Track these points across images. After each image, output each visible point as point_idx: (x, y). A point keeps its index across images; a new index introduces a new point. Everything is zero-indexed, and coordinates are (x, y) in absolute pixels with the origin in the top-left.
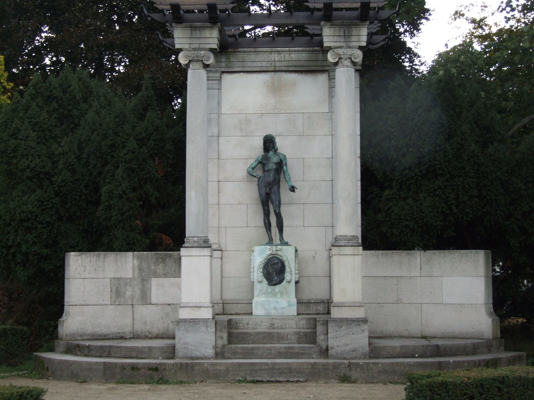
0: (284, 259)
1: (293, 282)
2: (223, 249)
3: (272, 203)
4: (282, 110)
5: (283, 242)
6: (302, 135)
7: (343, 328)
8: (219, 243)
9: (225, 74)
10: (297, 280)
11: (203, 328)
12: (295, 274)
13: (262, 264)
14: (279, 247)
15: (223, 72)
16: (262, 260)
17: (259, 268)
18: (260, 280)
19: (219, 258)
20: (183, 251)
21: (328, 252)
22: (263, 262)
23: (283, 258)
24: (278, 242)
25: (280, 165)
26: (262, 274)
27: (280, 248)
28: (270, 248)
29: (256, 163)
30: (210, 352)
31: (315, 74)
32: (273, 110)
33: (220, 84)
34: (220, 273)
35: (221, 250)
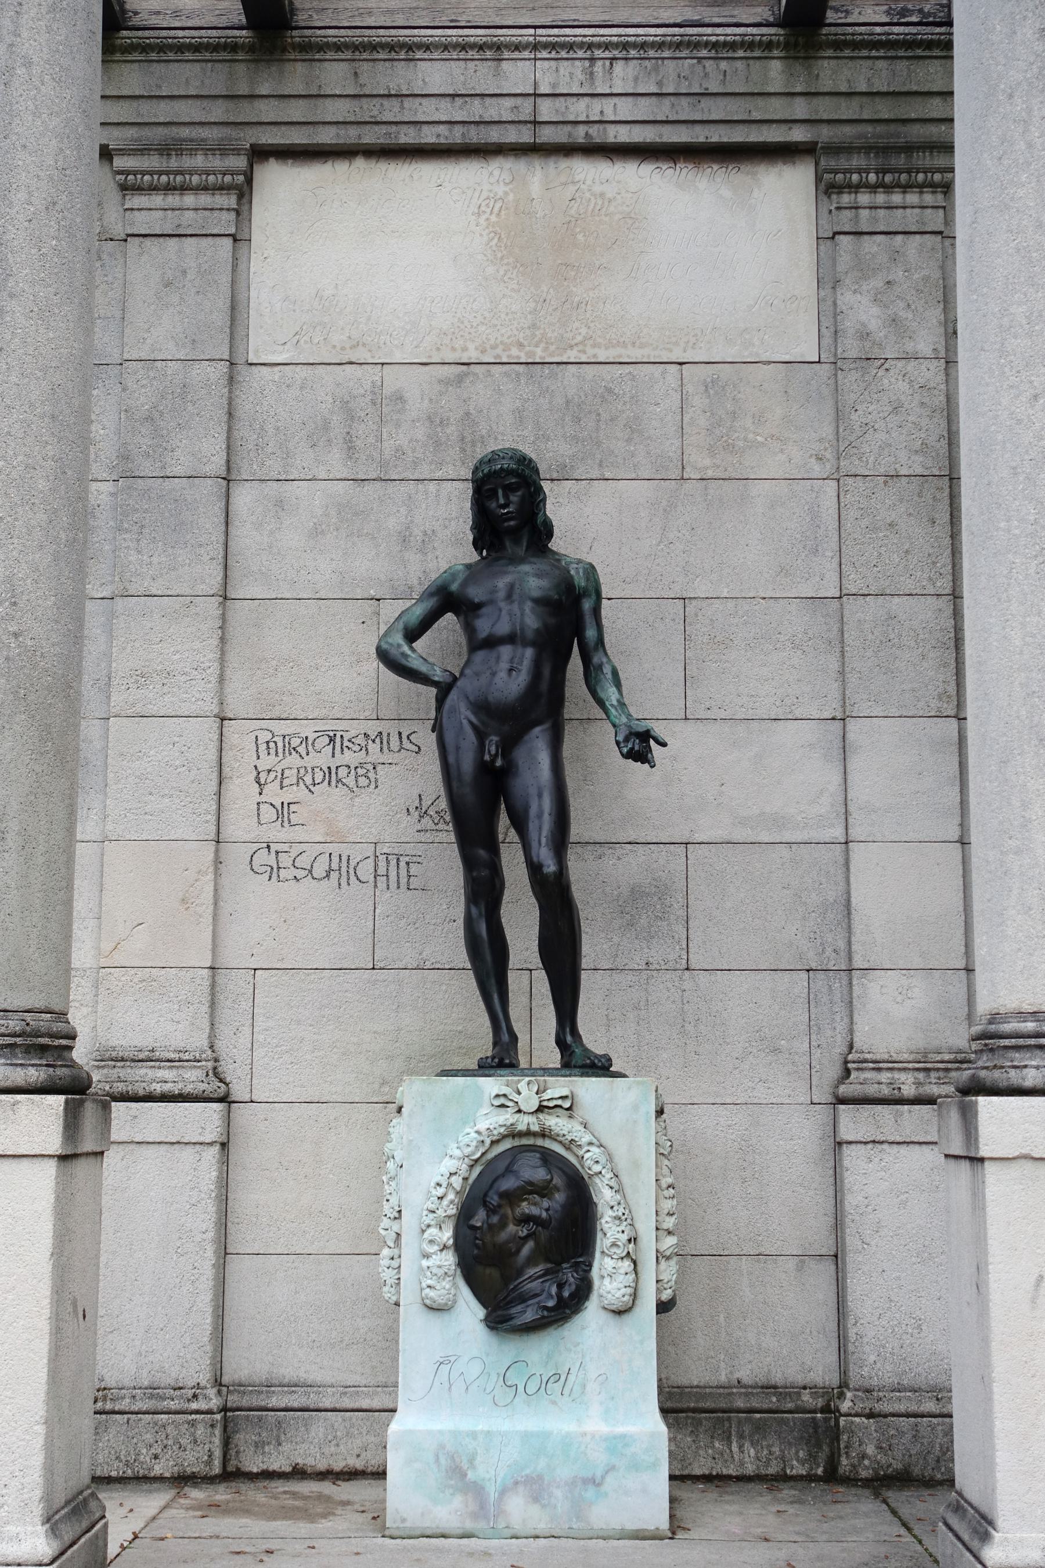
0: (591, 1161)
2: (238, 1091)
3: (519, 823)
4: (571, 347)
5: (578, 1059)
6: (676, 473)
8: (216, 1060)
9: (272, 160)
10: (666, 1296)
12: (660, 1256)
13: (451, 1196)
14: (558, 1088)
15: (260, 154)
17: (429, 1219)
19: (211, 1144)
21: (822, 1114)
22: (457, 1182)
24: (553, 1057)
26: (449, 1260)
27: (565, 1092)
28: (505, 1090)
31: (747, 167)
32: (521, 345)
33: (242, 211)
34: (211, 1235)
35: (221, 1100)
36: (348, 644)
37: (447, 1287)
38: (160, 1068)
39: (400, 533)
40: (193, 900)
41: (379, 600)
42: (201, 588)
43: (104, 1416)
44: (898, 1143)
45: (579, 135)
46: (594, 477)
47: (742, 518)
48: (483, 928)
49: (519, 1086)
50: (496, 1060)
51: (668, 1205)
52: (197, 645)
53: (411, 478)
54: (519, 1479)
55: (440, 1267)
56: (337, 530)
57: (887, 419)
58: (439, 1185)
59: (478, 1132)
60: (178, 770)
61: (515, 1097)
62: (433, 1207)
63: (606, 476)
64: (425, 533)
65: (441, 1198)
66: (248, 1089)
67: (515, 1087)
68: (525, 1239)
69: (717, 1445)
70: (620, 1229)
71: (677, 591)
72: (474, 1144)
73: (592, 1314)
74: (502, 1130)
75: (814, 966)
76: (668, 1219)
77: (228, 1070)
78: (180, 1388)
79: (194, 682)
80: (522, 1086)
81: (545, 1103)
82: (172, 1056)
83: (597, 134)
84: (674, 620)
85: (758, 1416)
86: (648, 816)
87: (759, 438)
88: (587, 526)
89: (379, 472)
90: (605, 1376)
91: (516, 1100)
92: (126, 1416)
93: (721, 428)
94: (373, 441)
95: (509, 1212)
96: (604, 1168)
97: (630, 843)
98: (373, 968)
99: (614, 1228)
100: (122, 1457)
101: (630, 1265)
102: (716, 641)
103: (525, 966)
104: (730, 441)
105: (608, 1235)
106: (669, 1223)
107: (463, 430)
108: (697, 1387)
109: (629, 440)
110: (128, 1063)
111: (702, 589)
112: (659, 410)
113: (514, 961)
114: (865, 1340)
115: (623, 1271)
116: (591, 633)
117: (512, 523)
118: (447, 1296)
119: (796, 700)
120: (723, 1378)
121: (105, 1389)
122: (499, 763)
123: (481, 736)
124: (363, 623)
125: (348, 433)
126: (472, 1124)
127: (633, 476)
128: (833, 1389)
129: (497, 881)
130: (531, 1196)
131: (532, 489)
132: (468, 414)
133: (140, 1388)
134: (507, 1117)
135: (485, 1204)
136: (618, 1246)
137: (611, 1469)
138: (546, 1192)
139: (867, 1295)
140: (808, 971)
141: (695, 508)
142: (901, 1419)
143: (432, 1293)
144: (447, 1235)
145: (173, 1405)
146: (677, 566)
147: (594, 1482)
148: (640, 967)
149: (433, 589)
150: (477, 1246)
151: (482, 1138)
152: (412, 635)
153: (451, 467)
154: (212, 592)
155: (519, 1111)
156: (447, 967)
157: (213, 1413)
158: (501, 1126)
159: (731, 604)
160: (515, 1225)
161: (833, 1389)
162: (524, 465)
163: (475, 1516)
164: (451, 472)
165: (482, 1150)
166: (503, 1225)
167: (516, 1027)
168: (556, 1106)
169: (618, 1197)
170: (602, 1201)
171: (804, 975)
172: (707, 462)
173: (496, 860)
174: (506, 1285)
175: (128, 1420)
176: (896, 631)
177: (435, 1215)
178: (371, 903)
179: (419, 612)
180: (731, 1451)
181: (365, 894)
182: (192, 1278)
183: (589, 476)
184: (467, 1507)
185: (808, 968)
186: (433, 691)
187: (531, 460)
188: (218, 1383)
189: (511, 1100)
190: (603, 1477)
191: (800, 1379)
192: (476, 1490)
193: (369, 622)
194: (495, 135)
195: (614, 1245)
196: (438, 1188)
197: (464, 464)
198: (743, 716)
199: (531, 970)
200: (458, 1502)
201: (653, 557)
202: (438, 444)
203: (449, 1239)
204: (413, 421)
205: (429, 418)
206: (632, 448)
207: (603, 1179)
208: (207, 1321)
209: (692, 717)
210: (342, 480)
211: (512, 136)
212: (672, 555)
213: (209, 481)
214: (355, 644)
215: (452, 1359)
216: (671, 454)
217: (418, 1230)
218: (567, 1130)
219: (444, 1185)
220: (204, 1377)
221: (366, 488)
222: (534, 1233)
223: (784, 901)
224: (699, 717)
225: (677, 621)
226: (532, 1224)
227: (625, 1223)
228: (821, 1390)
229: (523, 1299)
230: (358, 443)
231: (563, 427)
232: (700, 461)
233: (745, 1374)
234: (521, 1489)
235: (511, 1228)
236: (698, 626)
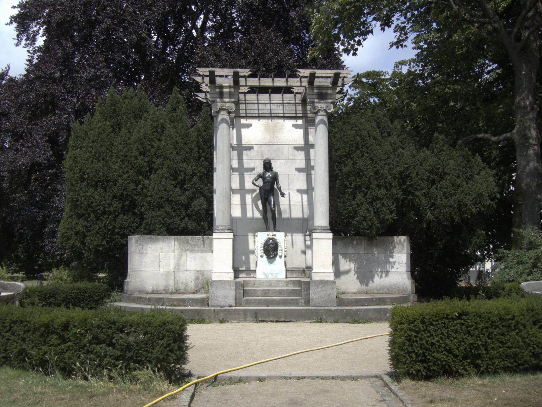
1: (283, 257)
7: (320, 287)
11: (228, 287)
18: (262, 254)
20: (215, 235)
25: (275, 178)
30: (233, 302)
45: (276, 115)
73: (278, 257)
83: (278, 115)
111: (290, 173)
152: (256, 181)
192: (266, 274)
194: (265, 115)
211: (267, 115)
232: (290, 157)
233: (294, 266)
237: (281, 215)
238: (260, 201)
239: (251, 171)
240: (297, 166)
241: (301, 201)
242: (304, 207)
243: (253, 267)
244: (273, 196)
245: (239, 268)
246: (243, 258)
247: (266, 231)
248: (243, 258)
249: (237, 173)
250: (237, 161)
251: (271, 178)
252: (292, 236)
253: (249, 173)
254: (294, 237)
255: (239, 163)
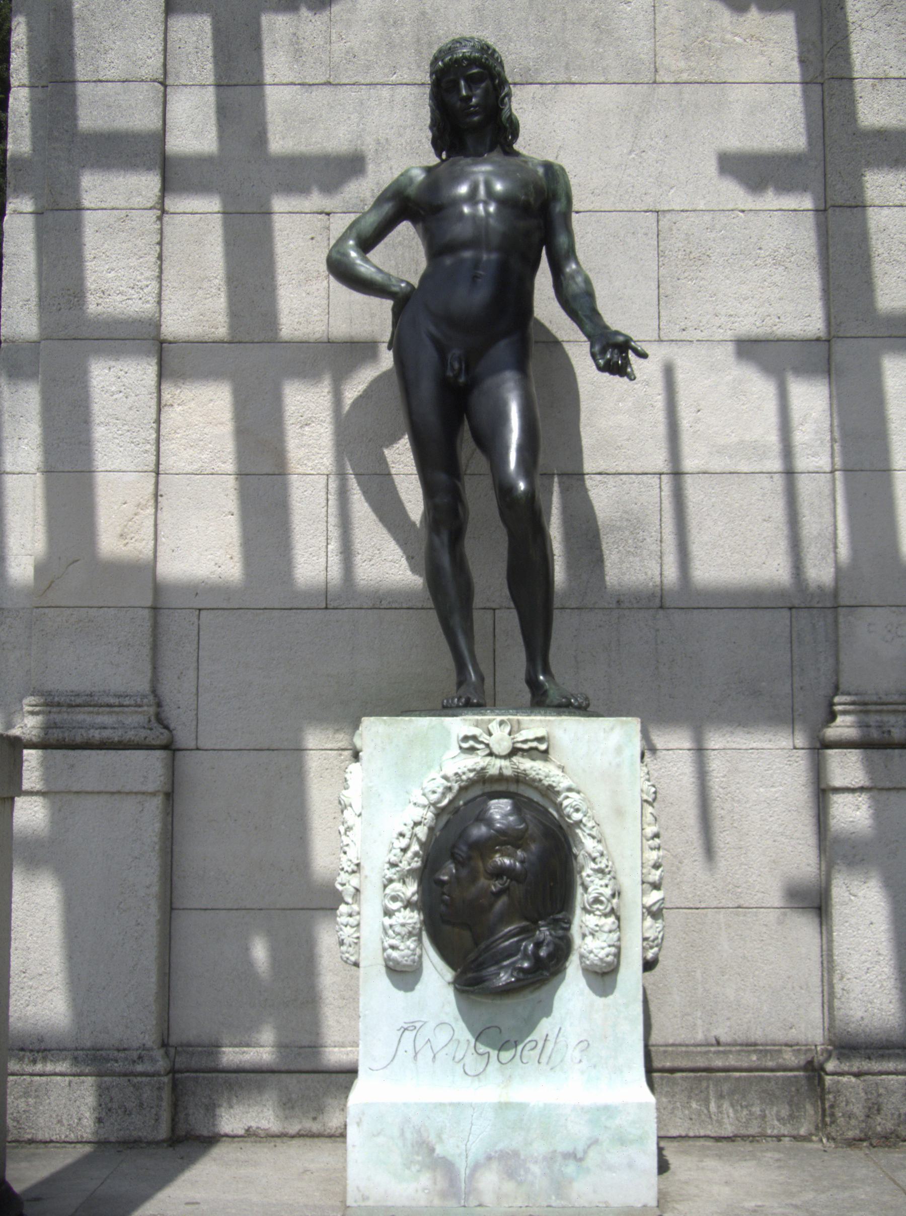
1: (631, 971)
2: (184, 738)
6: (648, 76)
10: (650, 955)
13: (415, 847)
16: (418, 814)
17: (391, 873)
18: (405, 950)
19: (154, 794)
22: (422, 832)
23: (559, 807)
26: (413, 917)
27: (540, 733)
28: (476, 731)
29: (387, 208)
34: (155, 889)
35: (165, 747)
36: (297, 262)
37: (412, 946)
38: (98, 713)
39: (351, 141)
40: (133, 535)
41: (328, 214)
42: (137, 201)
43: (44, 1078)
44: (889, 789)
46: (560, 80)
47: (719, 125)
48: (445, 560)
49: (490, 726)
50: (463, 700)
51: (653, 856)
52: (134, 262)
53: (363, 82)
54: (493, 1154)
55: (403, 925)
56: (284, 138)
57: (876, 18)
58: (402, 835)
59: (446, 778)
60: (115, 397)
61: (484, 738)
62: (394, 859)
63: (574, 80)
64: (378, 142)
65: (404, 850)
66: (194, 736)
67: (485, 726)
68: (498, 894)
69: (694, 1105)
70: (603, 882)
71: (649, 203)
72: (440, 790)
74: (471, 775)
75: (796, 603)
76: (654, 871)
77: (172, 715)
78: (125, 1049)
79: (130, 302)
80: (494, 727)
81: (519, 745)
82: (112, 701)
84: (646, 234)
85: (737, 1074)
86: (619, 444)
87: (737, 39)
88: (553, 133)
89: (328, 76)
90: (586, 1043)
91: (486, 741)
92: (67, 1078)
93: (696, 28)
94: (322, 43)
95: (480, 864)
96: (585, 816)
97: (600, 474)
98: (326, 608)
99: (597, 881)
100: (65, 1121)
101: (614, 923)
102: (692, 256)
103: (488, 605)
104: (706, 42)
105: (590, 890)
106: (655, 875)
107: (418, 30)
108: (673, 1045)
109: (598, 41)
110: (64, 709)
112: (629, 9)
113: (478, 601)
114: (852, 995)
115: (606, 928)
116: (562, 240)
117: (476, 119)
118: (412, 957)
119: (777, 320)
120: (700, 1037)
121: (45, 1050)
122: (462, 380)
123: (441, 350)
124: (312, 239)
125: (295, 34)
126: (438, 768)
127: (602, 79)
128: (816, 1046)
129: (460, 508)
130: (504, 847)
131: (497, 81)
132: (423, 13)
133: (82, 1049)
134: (478, 761)
135: (453, 857)
136: (601, 902)
137: (594, 1142)
138: (520, 842)
139: (853, 949)
140: (790, 608)
141: (668, 114)
142: (891, 1077)
143: (395, 954)
144: (410, 889)
145: (117, 1067)
146: (650, 176)
147: (573, 1156)
148: (611, 606)
149: (388, 194)
150: (443, 901)
151: (449, 784)
152: (367, 244)
153: (405, 70)
154: (149, 205)
155: (491, 754)
156: (405, 606)
157: (159, 1075)
158: (471, 771)
159: (707, 217)
160: (486, 878)
161: (816, 1046)
162: (487, 54)
163: (444, 1195)
164: (406, 76)
165: (449, 797)
166: (474, 879)
167: (483, 667)
168: (531, 749)
169: (600, 847)
170: (583, 852)
171: (786, 613)
172: (682, 64)
173: (459, 484)
174: (476, 944)
175: (70, 1082)
176: (886, 245)
177: (398, 869)
178: (323, 539)
179: (372, 220)
180: (709, 1112)
181: (317, 529)
182: (136, 934)
183: (553, 80)
184: (435, 1183)
185: (789, 605)
186: (389, 304)
187: (494, 51)
188: (164, 1045)
189: (482, 742)
190: (585, 1152)
191: (780, 1036)
192: (445, 1167)
193: (319, 238)
195: (597, 901)
196: (401, 838)
197: (419, 67)
198: (721, 338)
199: (494, 610)
200: (425, 1179)
201: (623, 167)
202: (391, 45)
203: (413, 895)
204: (365, 21)
205: (382, 18)
206: (601, 50)
207: (584, 829)
208: (152, 981)
209: (666, 339)
210: (287, 84)
212: (645, 165)
213: (145, 86)
214: (304, 262)
215: (418, 1025)
216: (642, 56)
217: (380, 886)
218: (544, 774)
219: (408, 834)
220: (150, 1039)
221: (314, 94)
222: (508, 888)
223: (765, 534)
224: (674, 338)
225: (650, 235)
226: (505, 878)
227: (609, 876)
228: (803, 1048)
229: (497, 959)
230: (306, 45)
231: (526, 27)
233: (723, 1032)
234: (494, 1165)
235: (483, 881)
236: (673, 241)
237: (599, 561)
238: (404, 444)
239: (330, 187)
240: (734, 143)
241: (773, 438)
242: (806, 487)
243: (335, 1055)
244: (521, 365)
245: (214, 1047)
246: (260, 952)
247: (447, 709)
248: (260, 952)
249: (212, 204)
250: (210, 94)
251: (504, 202)
252: (700, 751)
253: (316, 200)
254: (717, 765)
255: (224, 112)
